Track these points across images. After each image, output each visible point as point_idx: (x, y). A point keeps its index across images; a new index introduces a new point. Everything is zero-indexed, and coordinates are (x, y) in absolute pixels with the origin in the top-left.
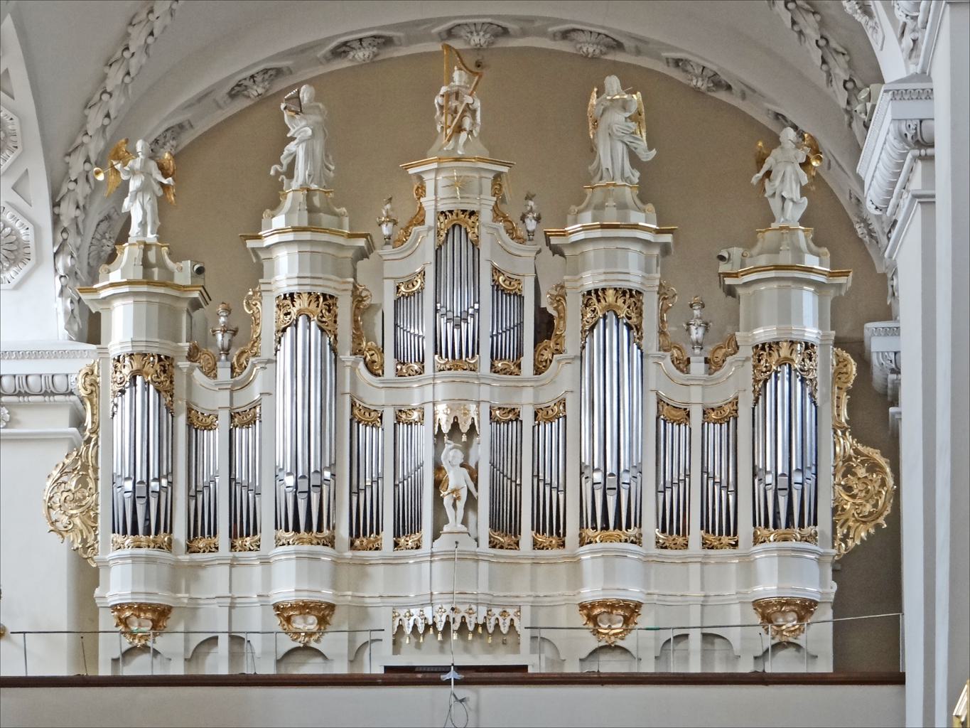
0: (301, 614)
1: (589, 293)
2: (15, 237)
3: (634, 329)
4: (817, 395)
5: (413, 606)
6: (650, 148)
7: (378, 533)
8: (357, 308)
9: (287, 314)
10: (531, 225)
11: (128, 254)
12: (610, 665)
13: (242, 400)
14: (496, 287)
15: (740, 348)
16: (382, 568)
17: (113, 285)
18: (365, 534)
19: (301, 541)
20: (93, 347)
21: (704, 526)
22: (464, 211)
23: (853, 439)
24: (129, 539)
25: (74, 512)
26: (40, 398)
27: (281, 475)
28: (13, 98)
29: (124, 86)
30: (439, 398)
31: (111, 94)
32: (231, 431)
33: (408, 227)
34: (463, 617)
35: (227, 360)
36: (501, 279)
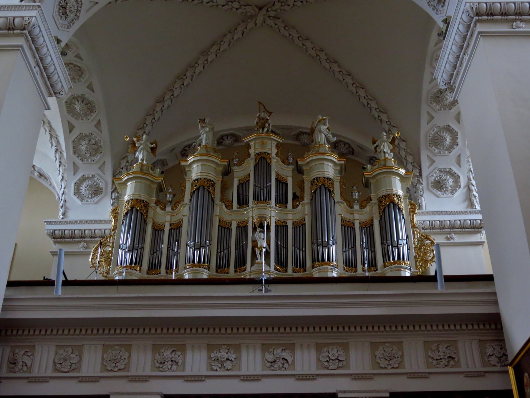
1: (314, 179)
2: (97, 186)
7: (228, 267)
13: (175, 219)
15: (373, 200)
18: (222, 267)
22: (265, 153)
28: (101, 132)
32: (170, 230)
35: (170, 204)
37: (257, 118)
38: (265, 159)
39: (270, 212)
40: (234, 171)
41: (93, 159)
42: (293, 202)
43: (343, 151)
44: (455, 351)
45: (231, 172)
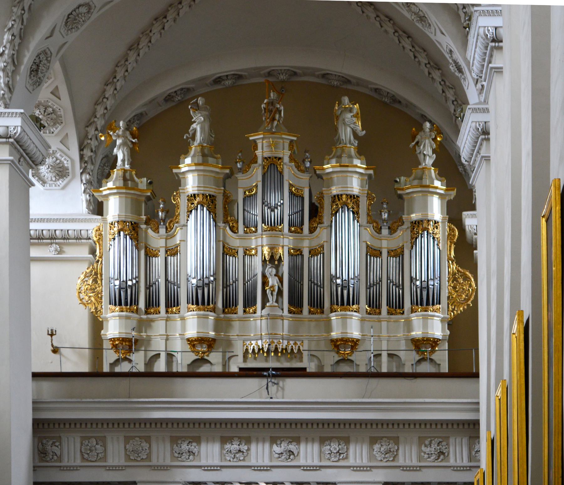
0: (199, 343)
1: (335, 196)
2: (61, 165)
3: (356, 213)
4: (440, 245)
5: (253, 340)
6: (363, 130)
7: (236, 306)
8: (226, 201)
9: (192, 204)
10: (308, 164)
11: (116, 173)
12: (345, 368)
13: (171, 243)
14: (291, 193)
15: (405, 223)
16: (238, 322)
17: (109, 189)
18: (230, 306)
19: (199, 310)
20: (100, 217)
21: (388, 304)
22: (276, 158)
23: (457, 265)
24: (118, 308)
25: (91, 295)
26: (74, 241)
27: (190, 278)
29: (114, 95)
30: (265, 244)
31: (107, 99)
32: (166, 258)
33: (249, 164)
34: (276, 345)
35: (164, 224)
36: (293, 189)
39: (281, 240)
40: (238, 178)
41: (52, 130)
43: (386, 100)
44: (447, 446)
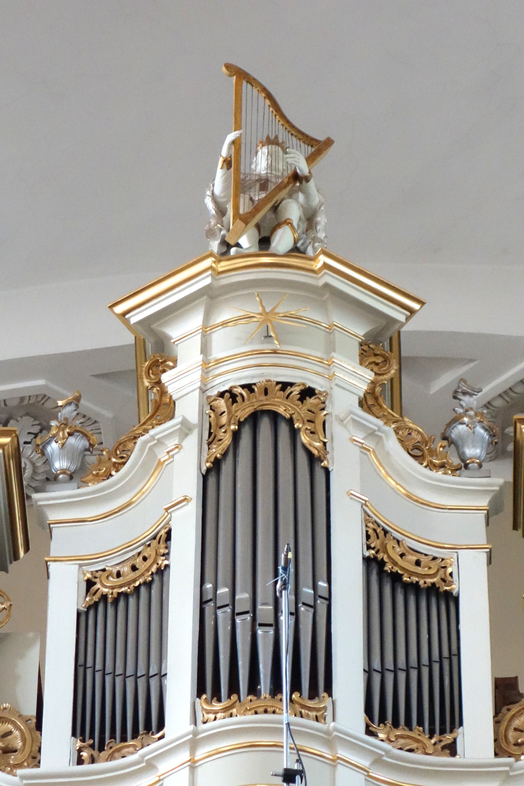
22: (285, 386)
37: (220, 173)
38: (284, 430)
40: (53, 516)
42: (497, 723)
45: (27, 549)
